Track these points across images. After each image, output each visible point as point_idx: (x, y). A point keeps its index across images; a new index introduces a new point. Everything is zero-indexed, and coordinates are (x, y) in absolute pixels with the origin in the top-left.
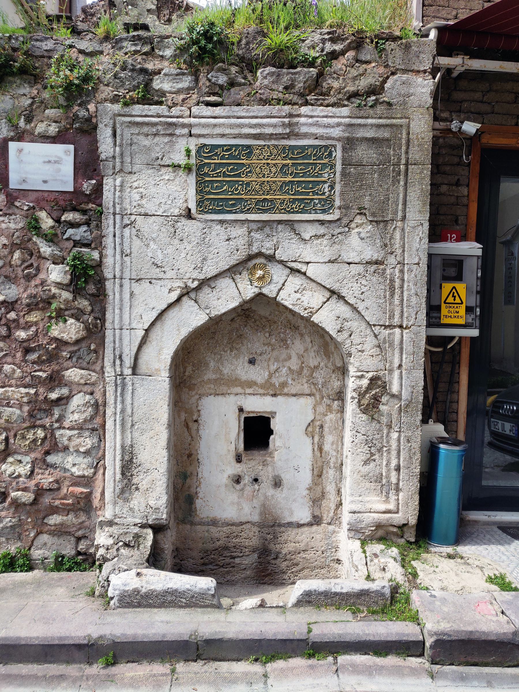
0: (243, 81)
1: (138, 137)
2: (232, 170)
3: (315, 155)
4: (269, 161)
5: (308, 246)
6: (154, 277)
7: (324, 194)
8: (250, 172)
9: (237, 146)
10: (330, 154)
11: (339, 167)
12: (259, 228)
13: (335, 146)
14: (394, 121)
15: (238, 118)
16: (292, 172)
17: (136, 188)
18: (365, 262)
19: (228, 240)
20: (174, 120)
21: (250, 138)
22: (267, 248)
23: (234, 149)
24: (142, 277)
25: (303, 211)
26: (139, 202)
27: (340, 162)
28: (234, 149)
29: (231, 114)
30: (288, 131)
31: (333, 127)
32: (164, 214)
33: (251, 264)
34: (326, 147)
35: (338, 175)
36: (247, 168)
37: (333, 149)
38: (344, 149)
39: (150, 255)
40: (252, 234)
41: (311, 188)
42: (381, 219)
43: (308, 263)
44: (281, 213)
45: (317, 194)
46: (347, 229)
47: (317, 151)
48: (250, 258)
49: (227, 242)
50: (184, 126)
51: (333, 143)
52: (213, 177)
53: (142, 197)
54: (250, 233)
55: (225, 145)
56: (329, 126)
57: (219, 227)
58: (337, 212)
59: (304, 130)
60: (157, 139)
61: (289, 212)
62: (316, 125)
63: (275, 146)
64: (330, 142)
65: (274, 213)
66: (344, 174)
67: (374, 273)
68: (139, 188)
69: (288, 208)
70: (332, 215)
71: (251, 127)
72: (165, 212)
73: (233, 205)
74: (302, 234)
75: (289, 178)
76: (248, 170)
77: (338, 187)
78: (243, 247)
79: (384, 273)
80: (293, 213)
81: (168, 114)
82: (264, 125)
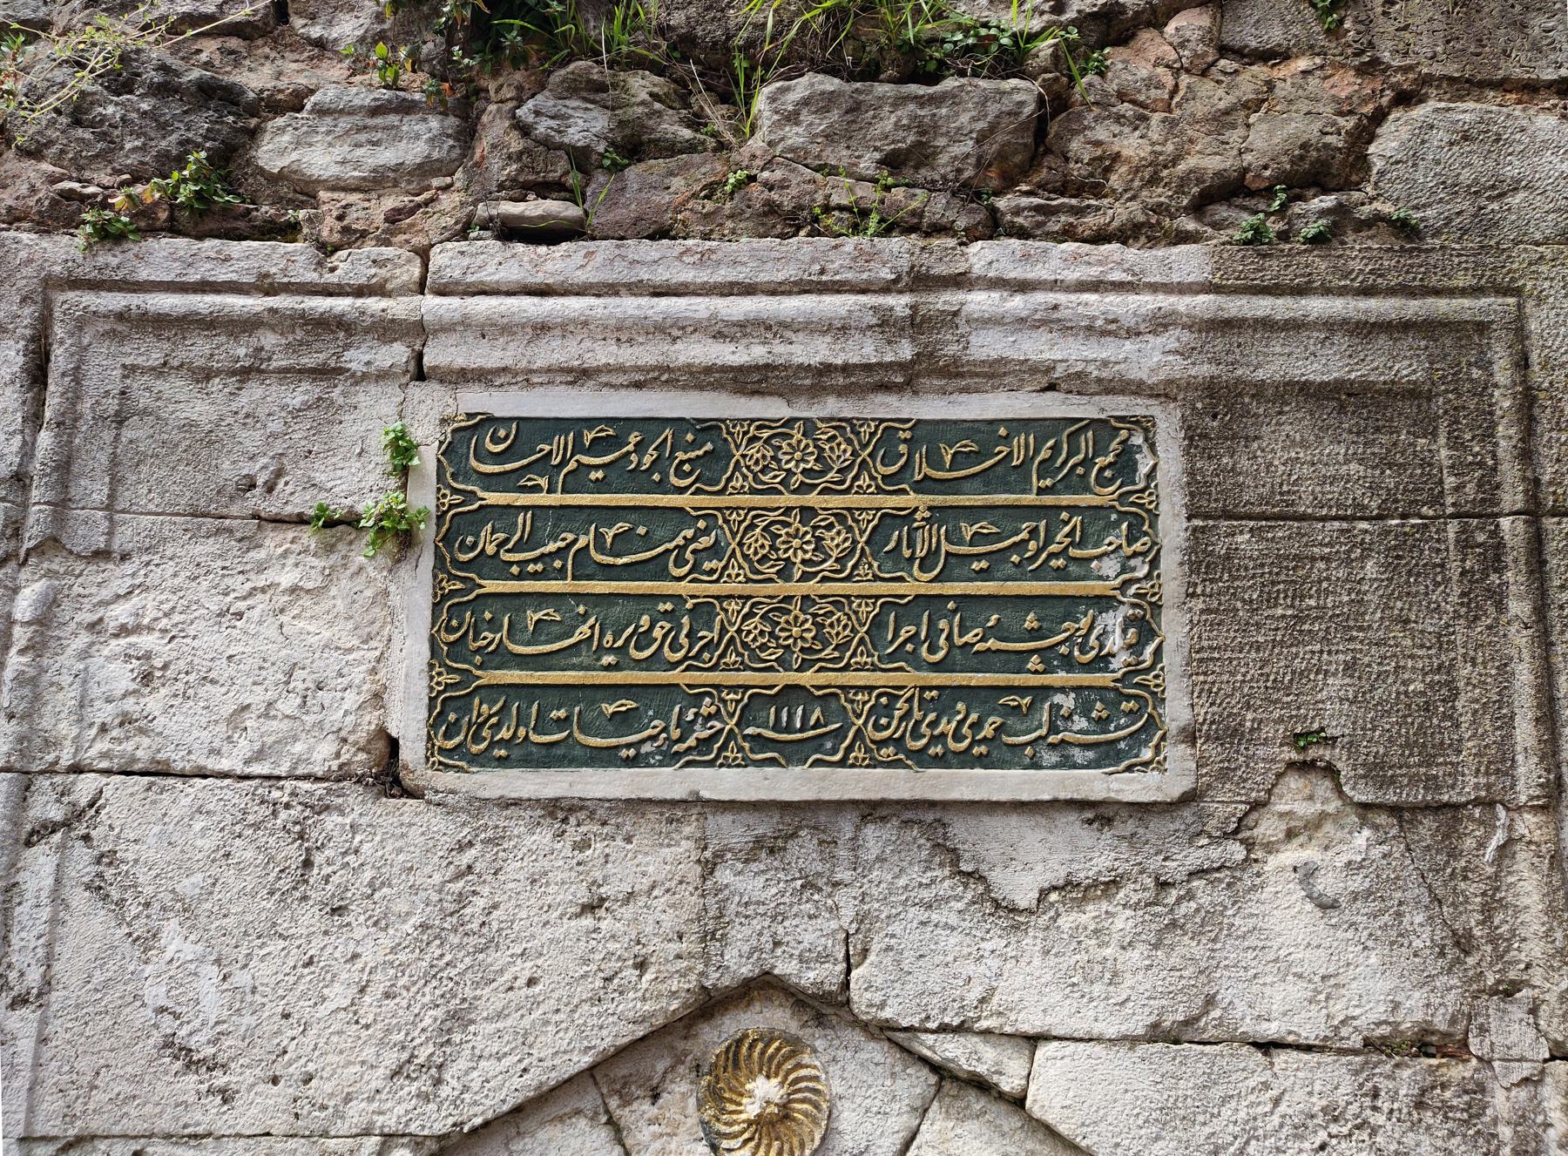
0: (687, 133)
1: (159, 385)
2: (624, 542)
3: (1046, 468)
4: (812, 499)
5: (1031, 942)
6: (164, 1124)
8: (715, 551)
9: (650, 425)
10: (1125, 464)
11: (1172, 528)
12: (759, 842)
13: (1146, 426)
14: (1442, 306)
15: (658, 292)
16: (933, 554)
17: (123, 631)
18: (1356, 1041)
19: (589, 908)
20: (342, 304)
21: (717, 386)
22: (805, 951)
23: (634, 438)
24: (96, 1125)
25: (996, 755)
26: (129, 705)
27: (1180, 499)
28: (634, 438)
29: (620, 273)
30: (906, 351)
32: (256, 769)
33: (715, 1037)
35: (1170, 563)
36: (700, 533)
37: (1138, 440)
38: (1195, 440)
39: (155, 994)
40: (724, 875)
41: (1035, 634)
42: (1420, 795)
43: (1033, 1040)
45: (1068, 663)
46: (1237, 851)
47: (1056, 449)
48: (710, 1005)
49: (587, 922)
50: (387, 330)
51: (1138, 407)
52: (520, 577)
53: (147, 678)
54: (709, 868)
55: (590, 422)
56: (1111, 329)
57: (543, 837)
58: (1179, 757)
59: (987, 346)
60: (254, 391)
61: (921, 759)
62: (1049, 322)
63: (841, 425)
64: (1119, 406)
65: (842, 763)
66: (1200, 561)
67: (1420, 1105)
68: (137, 629)
69: (916, 735)
70: (1153, 777)
71: (719, 336)
72: (259, 755)
73: (623, 721)
74: (995, 876)
76: (705, 541)
77: (1174, 629)
78: (675, 947)
79: (1475, 1111)
80: (941, 761)
81: (312, 277)
82: (784, 325)
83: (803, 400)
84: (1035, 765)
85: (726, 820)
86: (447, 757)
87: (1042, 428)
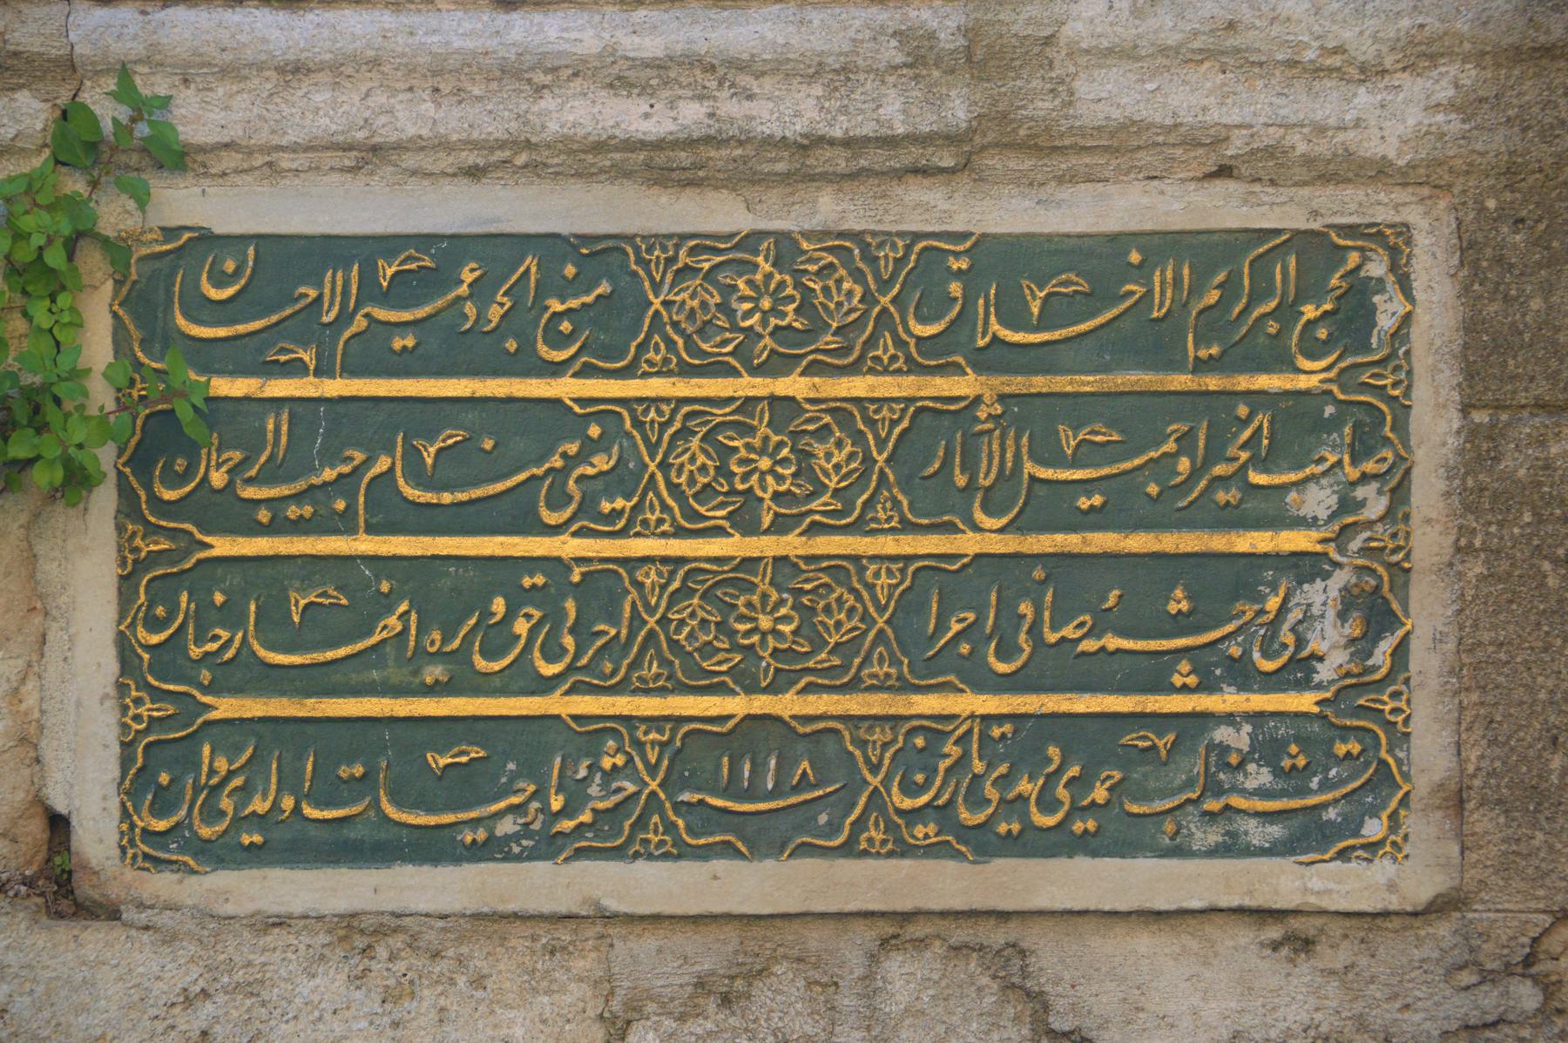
2: (459, 465)
3: (1212, 323)
4: (794, 385)
7: (1299, 671)
8: (620, 480)
11: (1434, 425)
13: (1394, 243)
16: (1009, 477)
21: (622, 173)
25: (1118, 838)
30: (958, 111)
31: (1370, 72)
34: (1315, 247)
35: (1429, 492)
37: (1377, 268)
44: (904, 850)
45: (1243, 676)
47: (1230, 288)
52: (277, 527)
55: (390, 244)
57: (330, 983)
58: (1422, 827)
61: (983, 844)
65: (849, 850)
69: (976, 799)
70: (1383, 869)
73: (467, 785)
75: (984, 537)
76: (602, 463)
83: (773, 197)
84: (1179, 851)
85: (647, 944)
86: (150, 850)
87: (1205, 250)
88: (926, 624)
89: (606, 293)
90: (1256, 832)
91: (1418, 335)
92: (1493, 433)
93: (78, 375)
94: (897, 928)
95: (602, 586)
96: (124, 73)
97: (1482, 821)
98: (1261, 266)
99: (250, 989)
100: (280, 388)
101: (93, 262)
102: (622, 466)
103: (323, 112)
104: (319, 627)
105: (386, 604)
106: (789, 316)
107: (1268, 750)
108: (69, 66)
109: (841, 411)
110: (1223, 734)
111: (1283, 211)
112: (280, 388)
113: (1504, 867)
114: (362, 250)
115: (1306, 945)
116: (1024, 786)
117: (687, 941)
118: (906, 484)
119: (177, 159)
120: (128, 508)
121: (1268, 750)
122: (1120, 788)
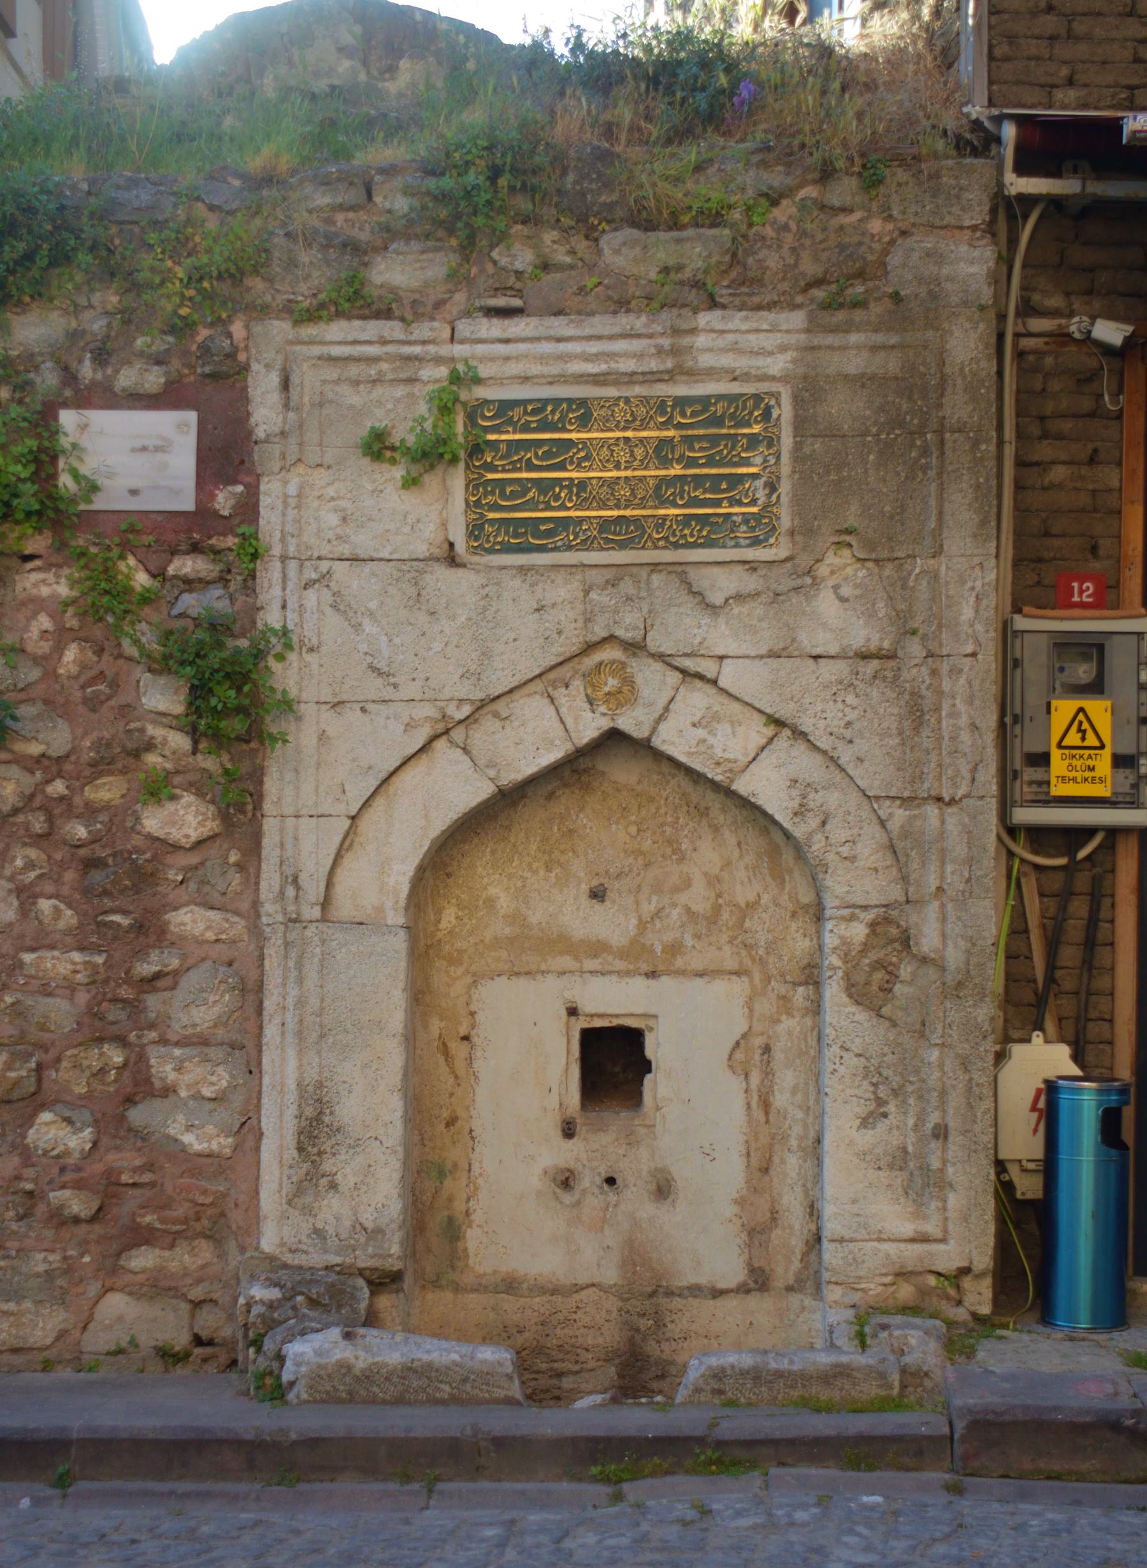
0: (568, 260)
1: (338, 389)
2: (547, 455)
3: (732, 416)
4: (629, 434)
5: (721, 620)
6: (370, 697)
7: (753, 502)
8: (587, 458)
9: (557, 402)
10: (767, 414)
11: (787, 441)
12: (607, 582)
13: (777, 396)
15: (559, 340)
16: (682, 456)
17: (333, 499)
18: (851, 654)
19: (537, 610)
20: (417, 350)
21: (587, 382)
22: (628, 625)
23: (549, 408)
24: (344, 697)
25: (710, 544)
26: (339, 531)
28: (549, 408)
29: (542, 332)
30: (669, 364)
31: (771, 353)
32: (394, 557)
33: (590, 662)
34: (757, 398)
35: (785, 458)
36: (579, 450)
37: (772, 402)
38: (797, 400)
39: (363, 647)
40: (593, 595)
42: (885, 554)
43: (722, 658)
44: (656, 548)
45: (740, 503)
46: (808, 580)
47: (737, 408)
48: (590, 648)
49: (536, 615)
50: (438, 360)
51: (774, 387)
52: (504, 471)
53: (344, 519)
54: (587, 593)
55: (530, 401)
56: (763, 352)
57: (517, 582)
58: (784, 540)
59: (706, 360)
60: (379, 391)
61: (676, 546)
62: (735, 349)
64: (764, 387)
65: (643, 548)
66: (798, 455)
67: (875, 677)
68: (339, 498)
69: (674, 535)
70: (774, 550)
72: (395, 551)
73: (549, 534)
74: (707, 593)
75: (676, 470)
76: (582, 454)
78: (573, 625)
79: (896, 678)
80: (684, 546)
81: (402, 337)
83: (624, 388)
84: (724, 547)
85: (594, 572)
86: (474, 550)
87: (731, 398)
88: (661, 492)
89: (584, 412)
90: (743, 542)
91: (783, 419)
92: (801, 443)
93: (456, 435)
94: (655, 567)
95: (582, 484)
96: (466, 361)
97: (798, 538)
98: (744, 402)
99: (497, 584)
100: (504, 437)
101: (458, 407)
102: (587, 454)
103: (514, 369)
104: (514, 495)
105: (530, 490)
106: (628, 417)
107: (746, 521)
108: (453, 359)
109: (641, 440)
110: (734, 518)
111: (749, 389)
112: (504, 437)
113: (804, 549)
114: (524, 402)
115: (755, 569)
116: (686, 532)
117: (603, 571)
118: (657, 457)
119: (478, 381)
120: (467, 467)
121: (746, 521)
122: (712, 531)
